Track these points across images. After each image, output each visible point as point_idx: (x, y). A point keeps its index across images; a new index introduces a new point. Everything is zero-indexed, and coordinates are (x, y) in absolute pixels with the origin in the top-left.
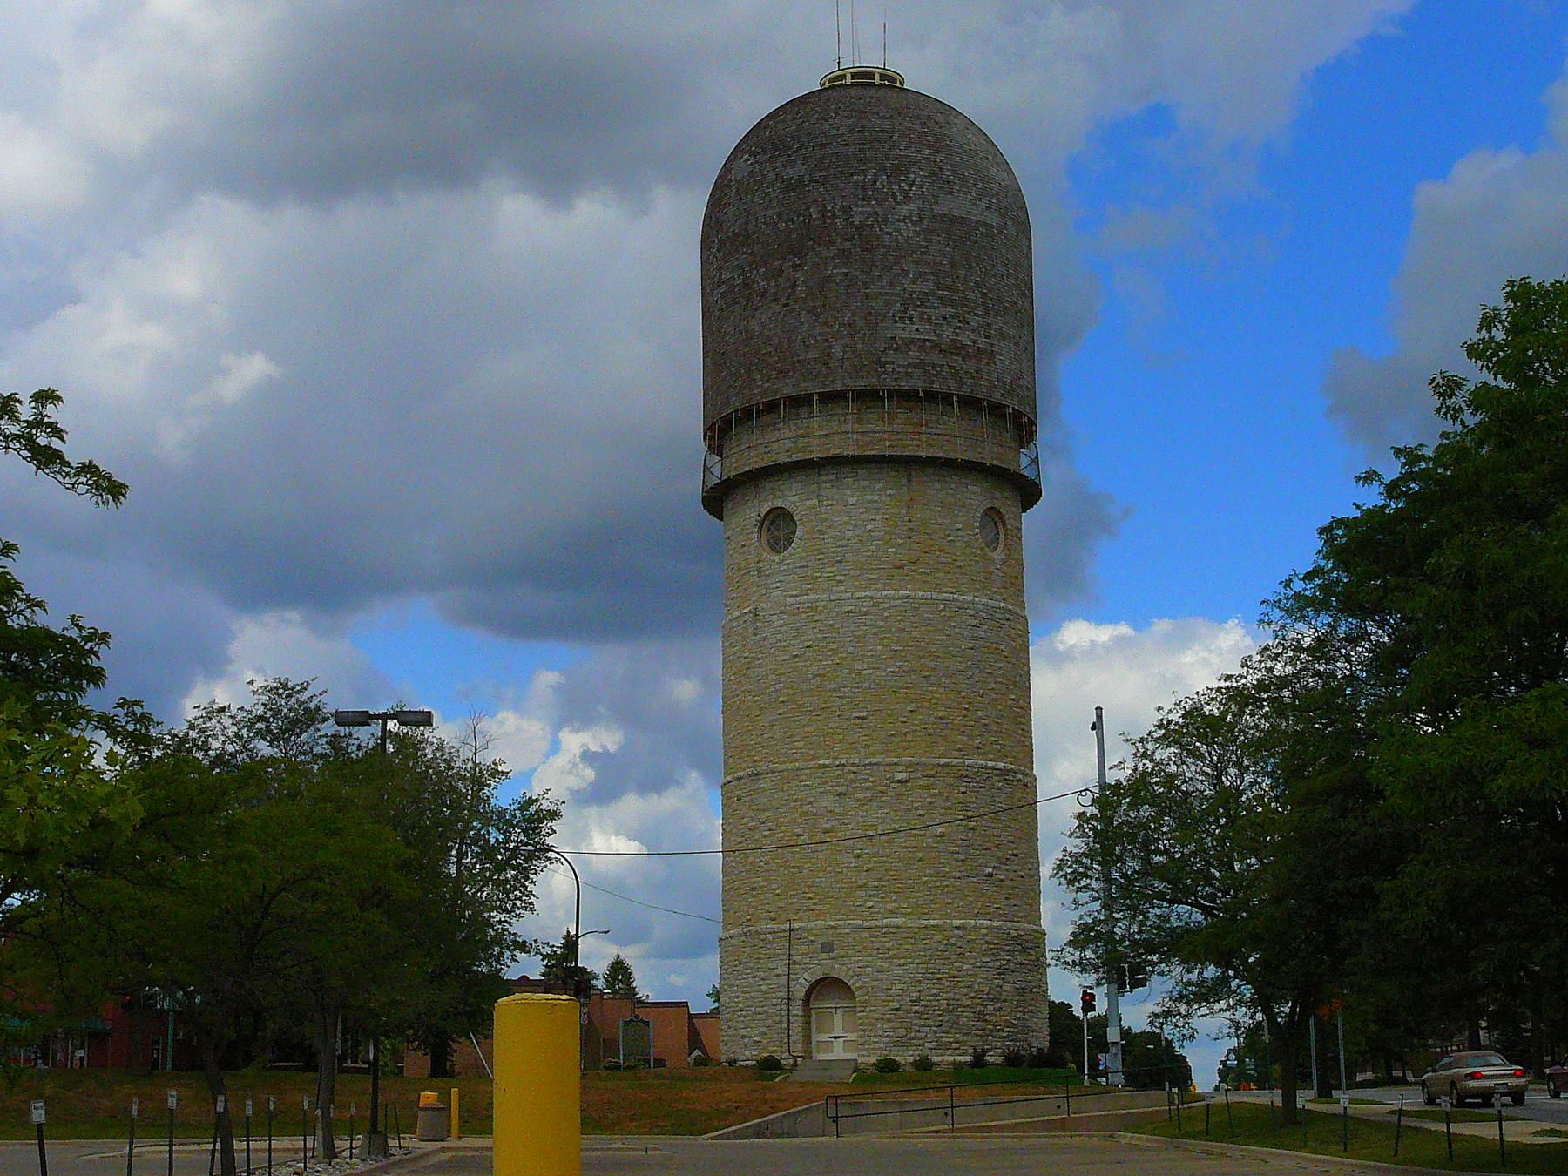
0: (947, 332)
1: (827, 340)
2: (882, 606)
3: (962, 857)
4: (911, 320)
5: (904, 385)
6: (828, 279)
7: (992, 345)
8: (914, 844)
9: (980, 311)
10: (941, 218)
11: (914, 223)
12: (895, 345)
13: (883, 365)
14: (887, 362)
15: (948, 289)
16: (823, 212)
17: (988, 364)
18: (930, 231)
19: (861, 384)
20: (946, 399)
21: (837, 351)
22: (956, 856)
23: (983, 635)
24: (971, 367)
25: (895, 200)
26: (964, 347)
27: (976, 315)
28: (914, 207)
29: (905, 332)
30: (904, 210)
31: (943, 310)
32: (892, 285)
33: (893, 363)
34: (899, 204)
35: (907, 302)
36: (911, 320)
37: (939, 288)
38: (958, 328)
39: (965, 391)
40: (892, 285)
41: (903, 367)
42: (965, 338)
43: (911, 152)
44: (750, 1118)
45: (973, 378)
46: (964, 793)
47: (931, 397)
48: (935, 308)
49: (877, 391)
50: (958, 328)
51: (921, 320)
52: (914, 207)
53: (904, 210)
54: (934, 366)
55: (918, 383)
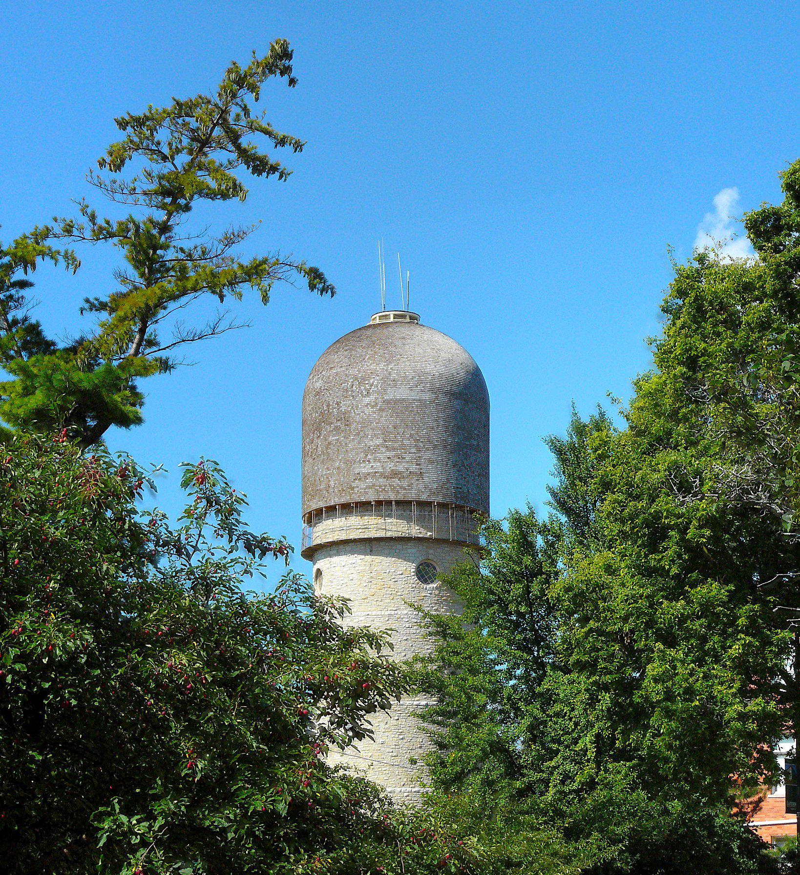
0: (390, 466)
1: (328, 478)
2: (355, 621)
3: (395, 754)
4: (369, 461)
5: (363, 499)
6: (329, 444)
7: (421, 469)
8: (368, 748)
9: (413, 450)
10: (387, 402)
11: (373, 407)
12: (360, 477)
13: (352, 489)
14: (354, 488)
15: (390, 441)
16: (328, 406)
17: (418, 480)
18: (381, 410)
19: (343, 501)
20: (389, 503)
21: (332, 483)
22: (391, 754)
23: (415, 631)
24: (405, 483)
25: (362, 395)
26: (401, 473)
27: (410, 453)
28: (372, 397)
29: (365, 469)
30: (367, 400)
31: (388, 454)
32: (359, 443)
33: (357, 487)
34: (365, 397)
35: (368, 451)
36: (369, 461)
37: (386, 441)
38: (397, 462)
39: (400, 497)
40: (359, 443)
41: (363, 489)
42: (401, 468)
43: (373, 367)
44: (771, 815)
45: (405, 489)
46: (398, 720)
47: (379, 503)
48: (383, 453)
49: (350, 503)
50: (397, 462)
51: (375, 460)
52: (372, 397)
53: (367, 400)
54: (380, 486)
55: (372, 497)
